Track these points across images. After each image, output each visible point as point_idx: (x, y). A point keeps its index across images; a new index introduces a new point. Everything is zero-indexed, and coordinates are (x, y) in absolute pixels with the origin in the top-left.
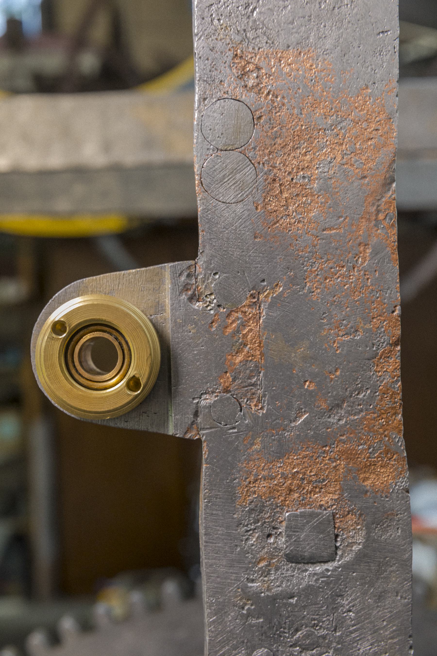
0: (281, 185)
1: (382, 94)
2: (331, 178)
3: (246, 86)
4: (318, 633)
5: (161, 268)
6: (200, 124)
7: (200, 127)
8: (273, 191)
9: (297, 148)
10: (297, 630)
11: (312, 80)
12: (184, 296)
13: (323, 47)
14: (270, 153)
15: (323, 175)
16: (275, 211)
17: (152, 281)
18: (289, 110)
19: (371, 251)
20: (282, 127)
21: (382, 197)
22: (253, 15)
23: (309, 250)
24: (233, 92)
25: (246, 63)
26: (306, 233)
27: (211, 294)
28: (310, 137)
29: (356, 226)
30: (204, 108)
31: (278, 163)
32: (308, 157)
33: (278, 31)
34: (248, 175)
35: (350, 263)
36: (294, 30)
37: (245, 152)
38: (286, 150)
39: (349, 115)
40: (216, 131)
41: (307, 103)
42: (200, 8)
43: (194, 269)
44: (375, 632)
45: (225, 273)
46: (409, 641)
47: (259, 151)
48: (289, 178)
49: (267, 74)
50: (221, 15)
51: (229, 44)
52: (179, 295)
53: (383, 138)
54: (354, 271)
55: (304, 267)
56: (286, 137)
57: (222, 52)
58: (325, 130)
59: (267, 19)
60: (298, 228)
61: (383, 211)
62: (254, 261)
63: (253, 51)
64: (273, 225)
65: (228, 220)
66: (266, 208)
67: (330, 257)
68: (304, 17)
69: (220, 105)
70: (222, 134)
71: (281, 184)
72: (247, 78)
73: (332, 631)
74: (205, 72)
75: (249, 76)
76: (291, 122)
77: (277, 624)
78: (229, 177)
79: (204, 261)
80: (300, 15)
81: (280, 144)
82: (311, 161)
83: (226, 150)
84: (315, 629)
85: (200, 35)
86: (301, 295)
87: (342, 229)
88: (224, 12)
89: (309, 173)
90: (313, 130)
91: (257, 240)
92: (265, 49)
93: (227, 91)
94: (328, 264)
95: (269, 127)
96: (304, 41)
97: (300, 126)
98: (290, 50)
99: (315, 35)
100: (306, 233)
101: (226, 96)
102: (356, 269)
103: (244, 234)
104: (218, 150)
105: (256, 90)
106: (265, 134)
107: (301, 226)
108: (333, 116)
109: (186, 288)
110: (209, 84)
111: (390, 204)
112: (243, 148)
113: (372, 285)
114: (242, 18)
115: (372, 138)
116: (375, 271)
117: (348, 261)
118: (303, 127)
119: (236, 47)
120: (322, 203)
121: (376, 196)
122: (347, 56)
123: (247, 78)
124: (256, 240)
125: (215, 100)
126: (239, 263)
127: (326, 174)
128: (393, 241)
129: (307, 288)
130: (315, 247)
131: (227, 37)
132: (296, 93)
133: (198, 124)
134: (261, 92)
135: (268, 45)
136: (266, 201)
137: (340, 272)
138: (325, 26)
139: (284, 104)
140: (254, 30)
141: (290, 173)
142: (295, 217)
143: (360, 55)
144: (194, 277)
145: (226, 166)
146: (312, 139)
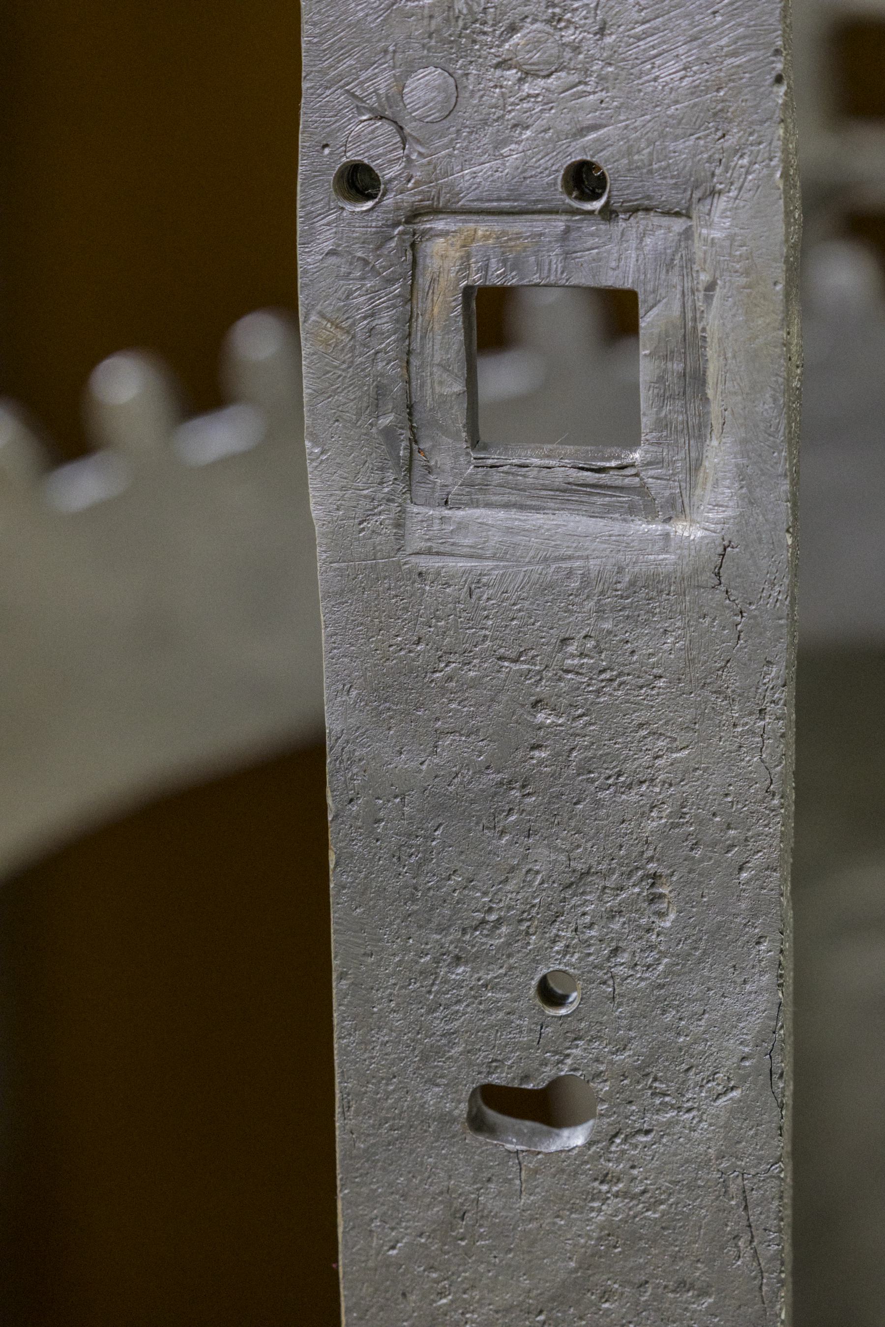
4: (562, 36)
10: (513, 29)
44: (694, 39)
46: (773, 62)
73: (595, 34)
77: (465, 11)
84: (555, 28)
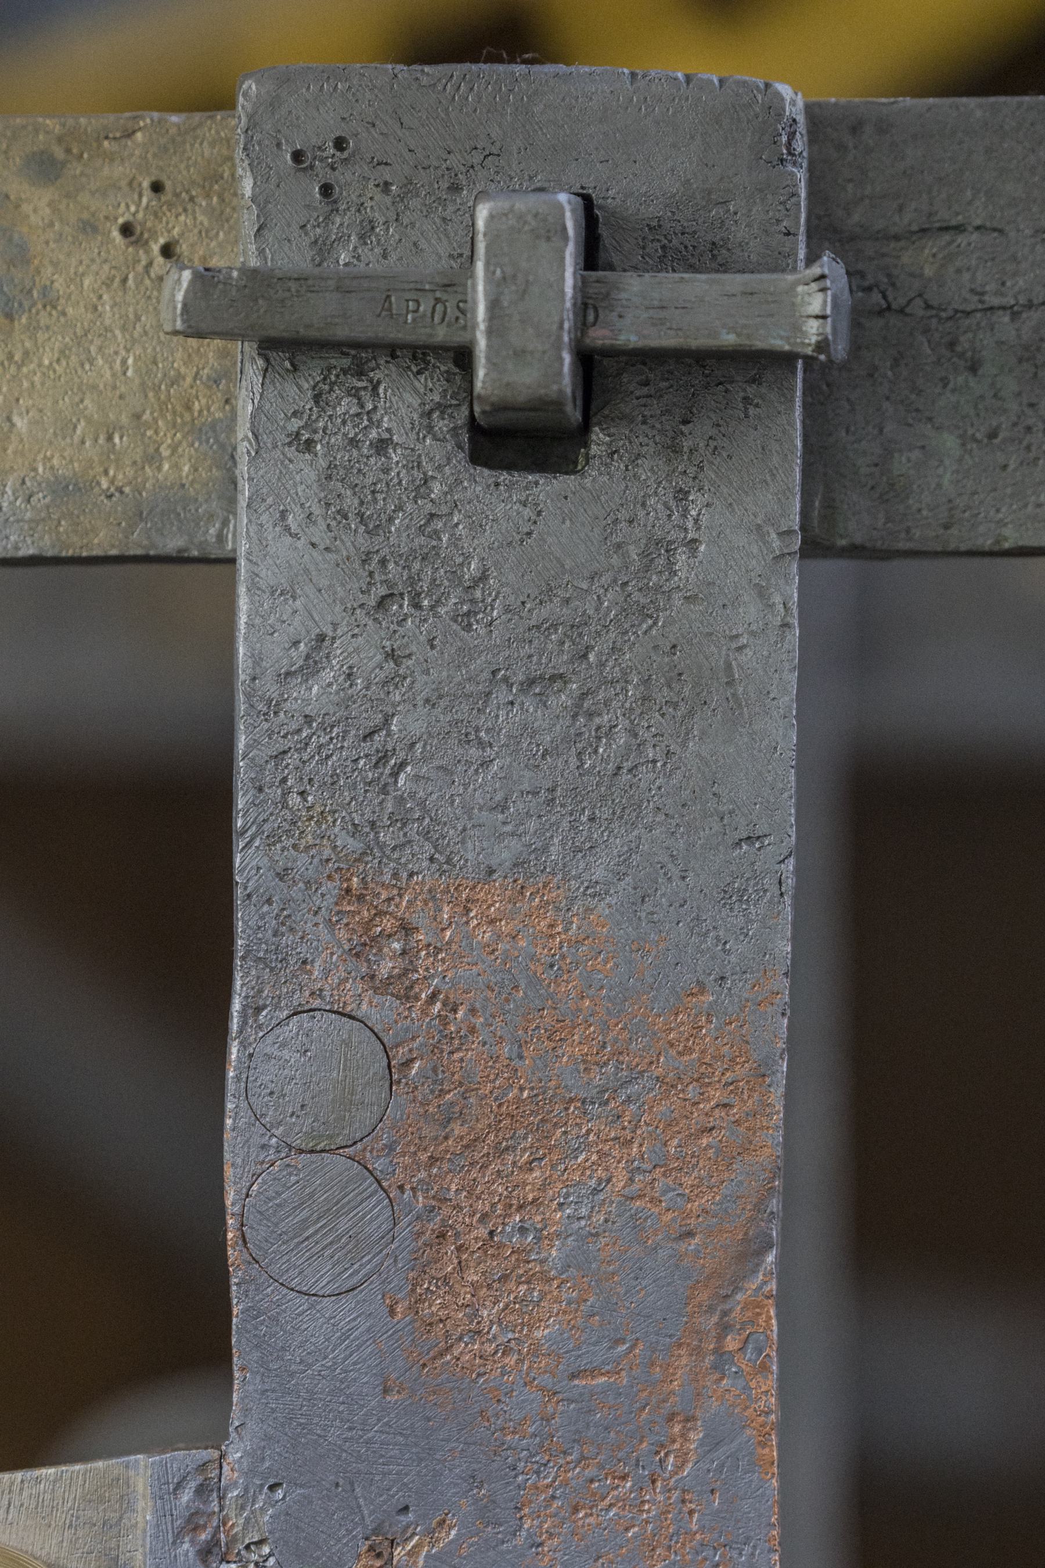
0: (459, 1249)
1: (742, 1009)
2: (597, 1235)
3: (373, 977)
5: (127, 1467)
6: (244, 1076)
7: (243, 1085)
8: (438, 1265)
9: (507, 1149)
11: (552, 966)
12: (186, 1546)
13: (586, 876)
14: (433, 1160)
15: (576, 1225)
16: (441, 1321)
17: (101, 1500)
18: (487, 1046)
19: (701, 1435)
20: (466, 1091)
21: (737, 1289)
22: (396, 782)
23: (531, 1430)
24: (335, 992)
25: (373, 912)
26: (526, 1384)
27: (261, 1542)
28: (542, 1120)
29: (661, 1366)
30: (256, 1033)
31: (454, 1187)
32: (537, 1173)
33: (464, 830)
34: (371, 1221)
35: (643, 1467)
36: (509, 828)
37: (364, 1157)
38: (477, 1156)
39: (652, 1063)
40: (287, 1099)
41: (538, 1027)
42: (253, 759)
43: (217, 1471)
45: (301, 1486)
47: (403, 1154)
48: (483, 1232)
49: (429, 945)
50: (310, 780)
51: (328, 860)
52: (174, 1543)
53: (742, 1129)
54: (654, 1490)
55: (516, 1476)
56: (478, 1120)
57: (308, 883)
58: (583, 1103)
59: (434, 796)
60: (503, 1367)
61: (738, 1327)
62: (382, 1456)
63: (394, 882)
64: (434, 1358)
65: (313, 1340)
66: (417, 1312)
67: (589, 1450)
68: (535, 793)
69: (300, 1027)
70: (302, 1106)
71: (462, 1246)
72: (375, 955)
74: (260, 935)
75: (380, 950)
76: (492, 1077)
78: (319, 1225)
79: (245, 1451)
80: (526, 786)
81: (462, 1138)
82: (544, 1185)
83: (312, 1152)
85: (249, 833)
86: (509, 1552)
87: (623, 1373)
88: (317, 773)
89: (539, 1218)
90: (551, 1101)
91: (392, 1398)
92: (426, 877)
93: (321, 990)
94: (583, 1469)
95: (432, 1092)
96: (533, 857)
97: (516, 1091)
98: (494, 881)
99: (563, 843)
100: (526, 1384)
101: (317, 1003)
102: (659, 1484)
103: (355, 1380)
104: (290, 1150)
105: (398, 988)
106: (421, 1110)
107: (512, 1363)
108: (606, 1064)
109: (192, 1524)
110: (272, 969)
111: (758, 1310)
112: (359, 1146)
113: (702, 1529)
114: (366, 791)
115: (713, 1128)
116: (712, 1491)
117: (638, 1461)
118: (525, 1094)
119: (349, 869)
120: (569, 1303)
121: (720, 1287)
122: (648, 906)
123: (375, 955)
124: (388, 1398)
125: (286, 1013)
126: (339, 1458)
127: (583, 1223)
128: (762, 1411)
129: (524, 1533)
130: (548, 1420)
131: (325, 841)
132: (507, 1000)
133: (238, 1078)
134: (412, 993)
135: (435, 866)
136: (419, 1291)
137: (616, 1493)
138: (592, 819)
139: (474, 1027)
140: (399, 825)
141: (484, 1217)
142: (495, 1337)
143: (685, 901)
144: (215, 1495)
145: (311, 1195)
146: (549, 1126)
